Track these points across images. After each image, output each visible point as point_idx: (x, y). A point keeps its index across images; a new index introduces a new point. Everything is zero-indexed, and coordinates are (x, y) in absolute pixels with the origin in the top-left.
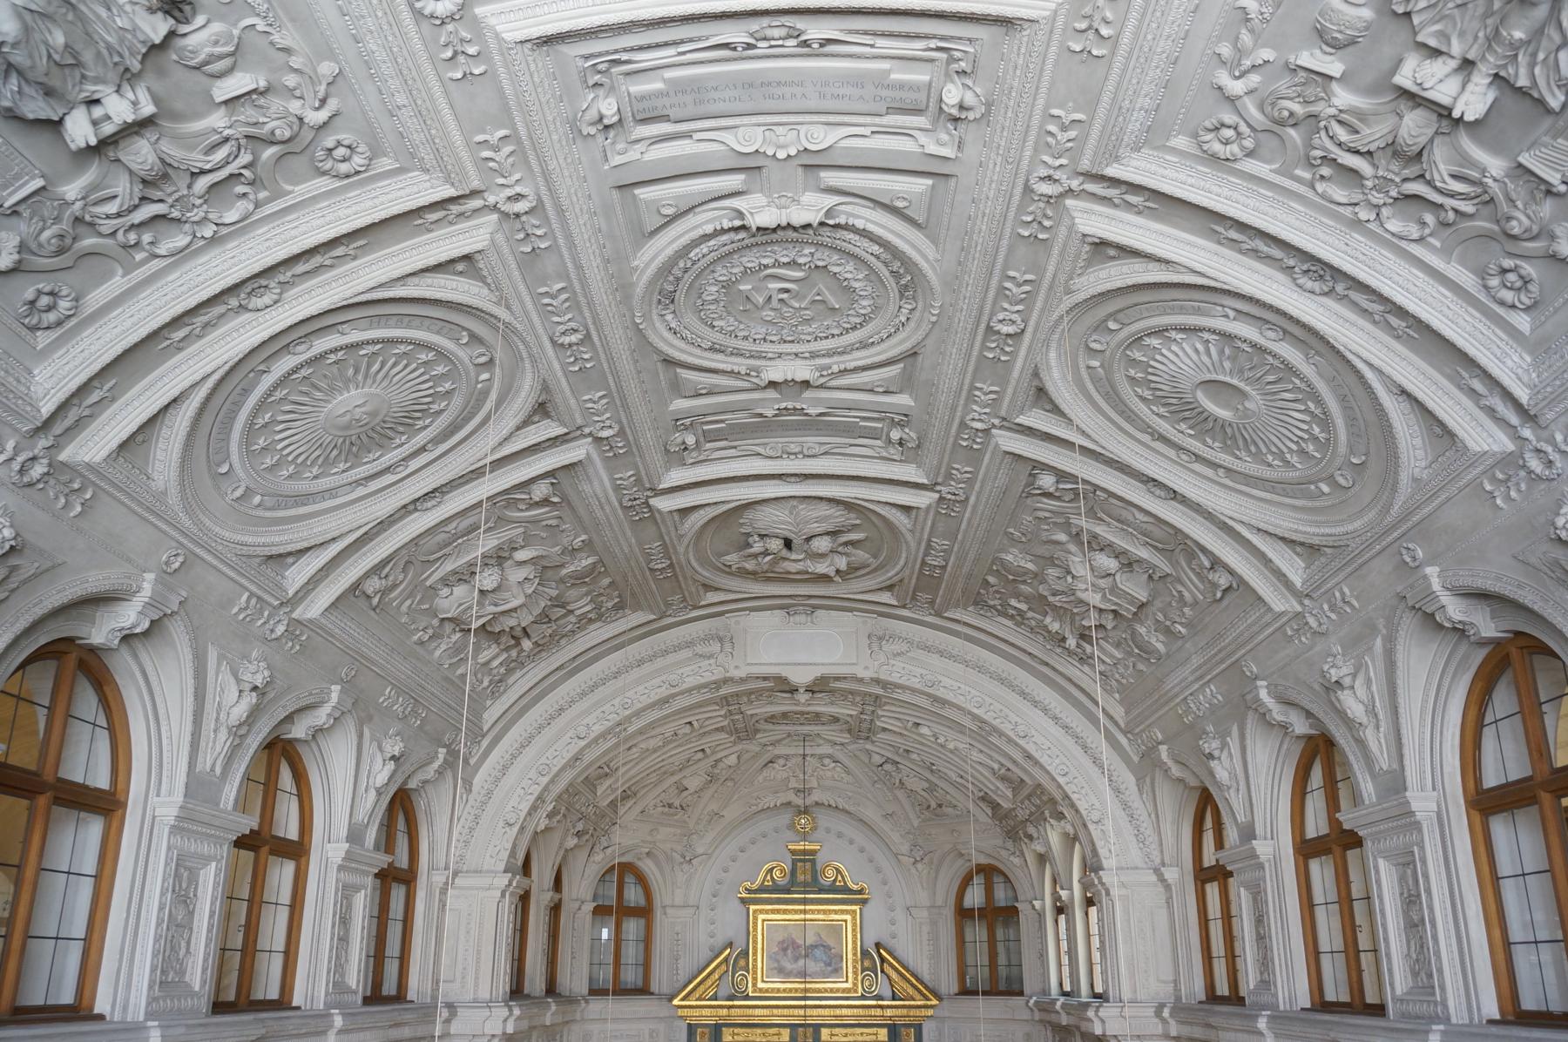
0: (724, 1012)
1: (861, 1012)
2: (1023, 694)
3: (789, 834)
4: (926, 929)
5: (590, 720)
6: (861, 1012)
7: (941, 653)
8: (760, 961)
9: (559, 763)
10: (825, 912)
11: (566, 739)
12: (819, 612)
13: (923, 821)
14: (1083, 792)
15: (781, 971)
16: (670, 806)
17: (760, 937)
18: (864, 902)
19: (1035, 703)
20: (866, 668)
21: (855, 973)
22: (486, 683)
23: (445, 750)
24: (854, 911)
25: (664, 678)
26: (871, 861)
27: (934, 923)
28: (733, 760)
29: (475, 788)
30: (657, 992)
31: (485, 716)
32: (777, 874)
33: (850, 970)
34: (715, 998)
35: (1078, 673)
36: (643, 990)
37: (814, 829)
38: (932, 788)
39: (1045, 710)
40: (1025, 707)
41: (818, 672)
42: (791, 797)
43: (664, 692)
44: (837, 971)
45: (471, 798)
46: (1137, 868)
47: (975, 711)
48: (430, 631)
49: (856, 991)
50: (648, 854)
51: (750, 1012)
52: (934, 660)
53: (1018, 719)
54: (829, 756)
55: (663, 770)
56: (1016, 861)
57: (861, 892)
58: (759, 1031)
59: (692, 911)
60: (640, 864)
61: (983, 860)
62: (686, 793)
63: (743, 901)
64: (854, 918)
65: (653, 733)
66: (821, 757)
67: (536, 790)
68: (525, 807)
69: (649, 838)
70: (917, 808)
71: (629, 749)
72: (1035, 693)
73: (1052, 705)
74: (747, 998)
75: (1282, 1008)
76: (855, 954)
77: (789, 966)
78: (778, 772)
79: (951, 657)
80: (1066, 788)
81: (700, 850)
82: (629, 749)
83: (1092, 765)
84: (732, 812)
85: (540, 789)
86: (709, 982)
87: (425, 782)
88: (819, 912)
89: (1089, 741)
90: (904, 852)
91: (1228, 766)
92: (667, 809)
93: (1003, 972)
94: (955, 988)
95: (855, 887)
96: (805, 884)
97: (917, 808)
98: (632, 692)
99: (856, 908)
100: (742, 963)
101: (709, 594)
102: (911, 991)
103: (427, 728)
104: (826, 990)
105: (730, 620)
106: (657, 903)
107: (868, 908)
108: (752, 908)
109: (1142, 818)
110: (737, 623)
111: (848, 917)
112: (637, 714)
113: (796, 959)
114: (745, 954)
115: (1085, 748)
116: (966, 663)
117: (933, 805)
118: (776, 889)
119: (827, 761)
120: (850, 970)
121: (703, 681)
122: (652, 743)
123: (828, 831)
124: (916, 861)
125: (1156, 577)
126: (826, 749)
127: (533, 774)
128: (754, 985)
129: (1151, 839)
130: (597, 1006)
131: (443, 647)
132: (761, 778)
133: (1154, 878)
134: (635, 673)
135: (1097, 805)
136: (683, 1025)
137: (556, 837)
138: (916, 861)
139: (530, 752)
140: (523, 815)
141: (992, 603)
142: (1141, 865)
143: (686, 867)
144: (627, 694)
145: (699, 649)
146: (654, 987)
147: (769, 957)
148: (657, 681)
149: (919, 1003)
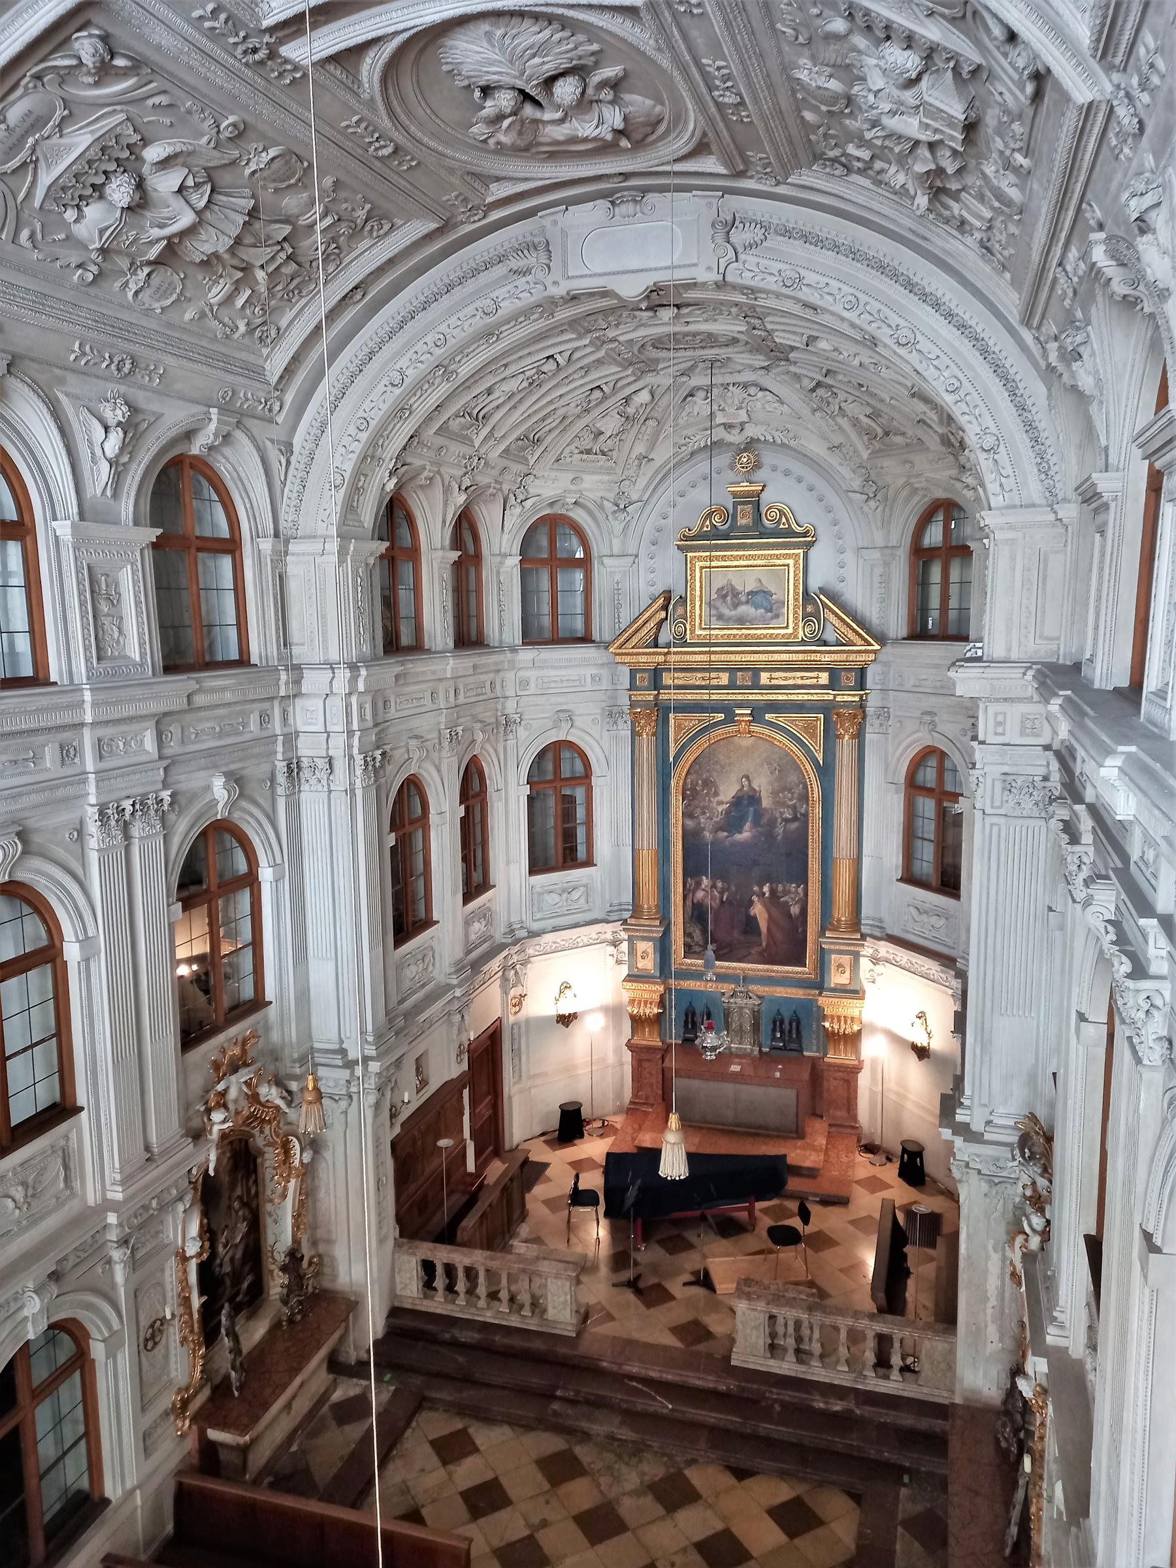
0: (661, 659)
1: (801, 657)
2: (910, 286)
3: (730, 475)
4: (878, 571)
5: (403, 363)
6: (801, 657)
7: (805, 238)
8: (697, 609)
9: (376, 417)
10: (765, 557)
11: (380, 388)
12: (652, 197)
13: (873, 453)
14: (977, 412)
15: (720, 617)
16: (588, 452)
17: (698, 585)
18: (810, 545)
19: (924, 297)
20: (709, 269)
21: (796, 618)
22: (242, 328)
23: (214, 411)
24: (797, 555)
25: (478, 304)
26: (821, 500)
27: (886, 564)
28: (644, 397)
29: (296, 449)
30: (598, 639)
31: (267, 366)
32: (716, 520)
33: (791, 616)
34: (656, 646)
35: (961, 247)
36: (586, 639)
37: (757, 466)
38: (874, 415)
39: (937, 305)
40: (911, 302)
41: (649, 280)
42: (719, 434)
43: (479, 322)
44: (777, 616)
45: (293, 459)
46: (1033, 505)
47: (846, 314)
48: (95, 269)
49: (796, 636)
50: (575, 503)
51: (688, 658)
52: (797, 249)
53: (902, 323)
54: (755, 385)
55: (560, 412)
56: (969, 494)
57: (805, 535)
58: (699, 675)
59: (631, 559)
60: (570, 514)
61: (940, 494)
62: (602, 438)
63: (679, 547)
64: (796, 562)
65: (508, 372)
66: (745, 386)
67: (358, 447)
68: (349, 467)
69: (573, 487)
70: (866, 438)
71: (489, 392)
72: (925, 283)
73: (946, 299)
74: (685, 644)
75: (1097, 686)
76: (796, 600)
77: (726, 612)
78: (700, 405)
79: (819, 242)
80: (954, 408)
81: (635, 497)
82: (489, 392)
83: (992, 375)
84: (663, 454)
85: (361, 446)
86: (645, 630)
87: (211, 448)
88: (759, 557)
89: (991, 343)
90: (857, 489)
91: (1091, 369)
92: (585, 456)
93: (952, 615)
94: (903, 632)
95: (799, 530)
96: (747, 528)
97: (866, 438)
98: (444, 326)
99: (801, 551)
100: (680, 611)
101: (493, 187)
102: (851, 635)
103: (178, 386)
104: (765, 636)
105: (544, 220)
106: (595, 553)
107: (813, 553)
108: (689, 555)
109: (1048, 443)
110: (555, 222)
111: (791, 562)
112: (463, 350)
113: (735, 606)
114: (683, 600)
115: (985, 352)
116: (836, 247)
117: (880, 431)
118: (716, 534)
119: (752, 390)
120: (791, 616)
121: (519, 304)
122: (512, 385)
123: (774, 469)
124: (869, 498)
125: (966, 70)
126: (747, 376)
127: (352, 430)
128: (693, 632)
129: (1056, 468)
130: (527, 655)
131: (133, 287)
132: (684, 414)
133: (1052, 517)
134: (445, 302)
135: (993, 429)
136: (626, 670)
137: (438, 492)
138: (869, 498)
139: (346, 405)
140: (347, 476)
141: (831, 154)
142: (1038, 501)
143: (622, 516)
144: (443, 328)
145: (514, 264)
146: (596, 636)
147: (710, 604)
148: (470, 310)
149: (863, 648)
